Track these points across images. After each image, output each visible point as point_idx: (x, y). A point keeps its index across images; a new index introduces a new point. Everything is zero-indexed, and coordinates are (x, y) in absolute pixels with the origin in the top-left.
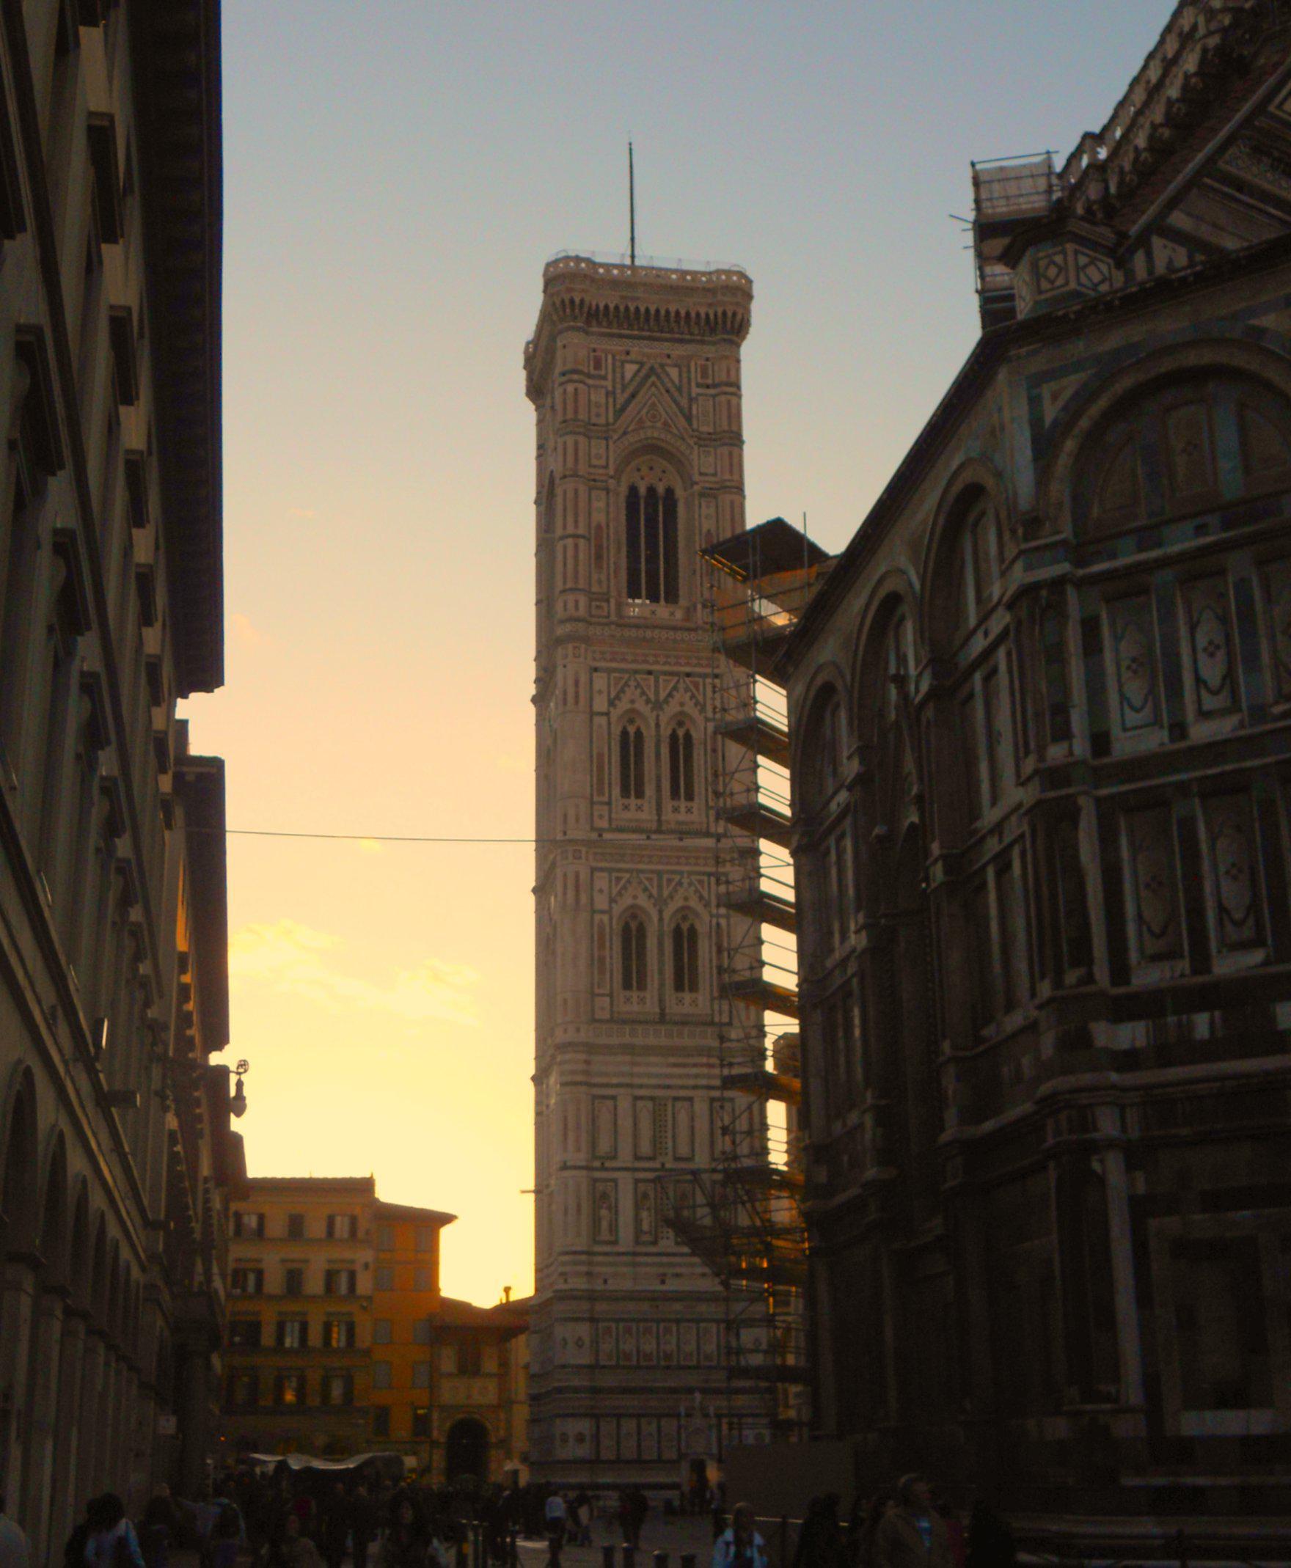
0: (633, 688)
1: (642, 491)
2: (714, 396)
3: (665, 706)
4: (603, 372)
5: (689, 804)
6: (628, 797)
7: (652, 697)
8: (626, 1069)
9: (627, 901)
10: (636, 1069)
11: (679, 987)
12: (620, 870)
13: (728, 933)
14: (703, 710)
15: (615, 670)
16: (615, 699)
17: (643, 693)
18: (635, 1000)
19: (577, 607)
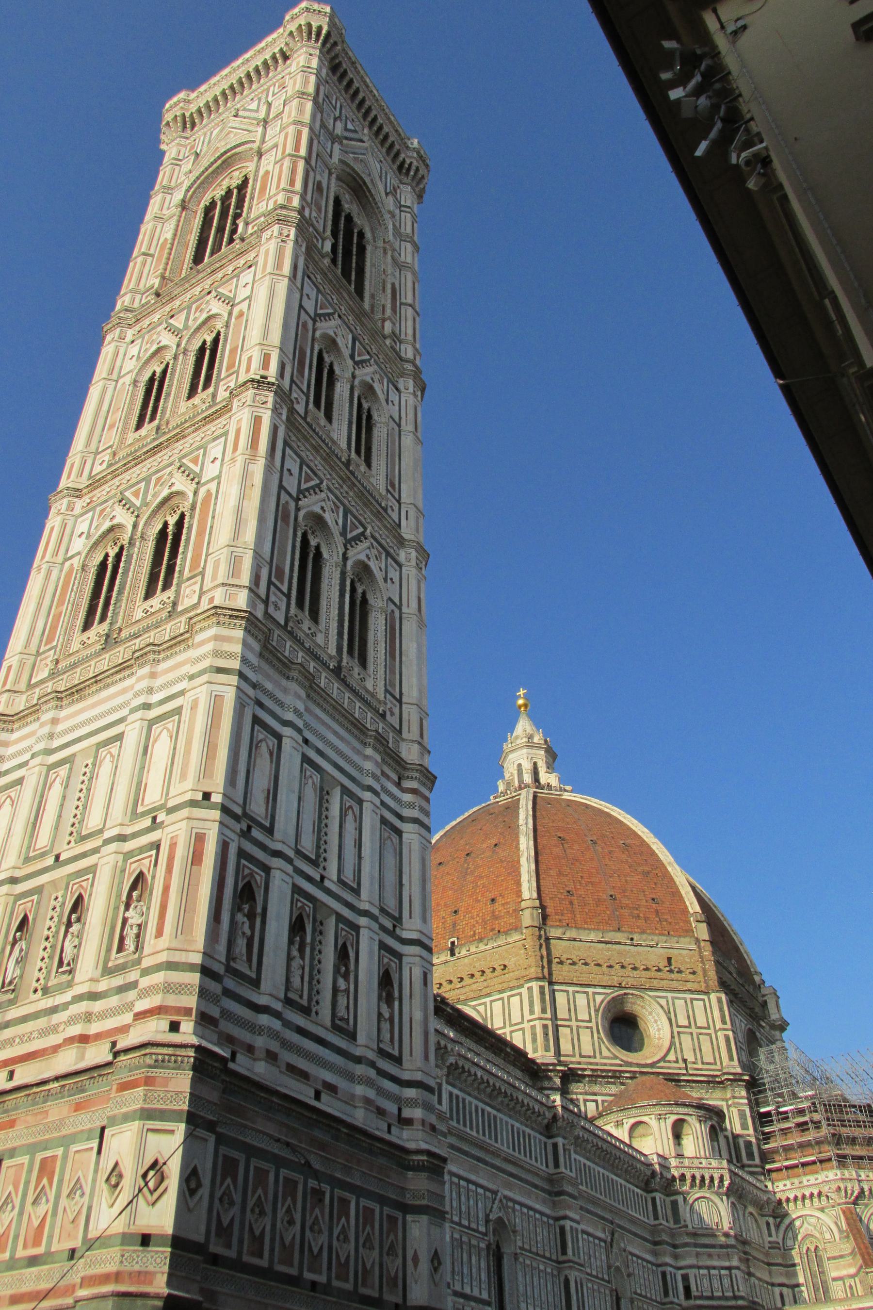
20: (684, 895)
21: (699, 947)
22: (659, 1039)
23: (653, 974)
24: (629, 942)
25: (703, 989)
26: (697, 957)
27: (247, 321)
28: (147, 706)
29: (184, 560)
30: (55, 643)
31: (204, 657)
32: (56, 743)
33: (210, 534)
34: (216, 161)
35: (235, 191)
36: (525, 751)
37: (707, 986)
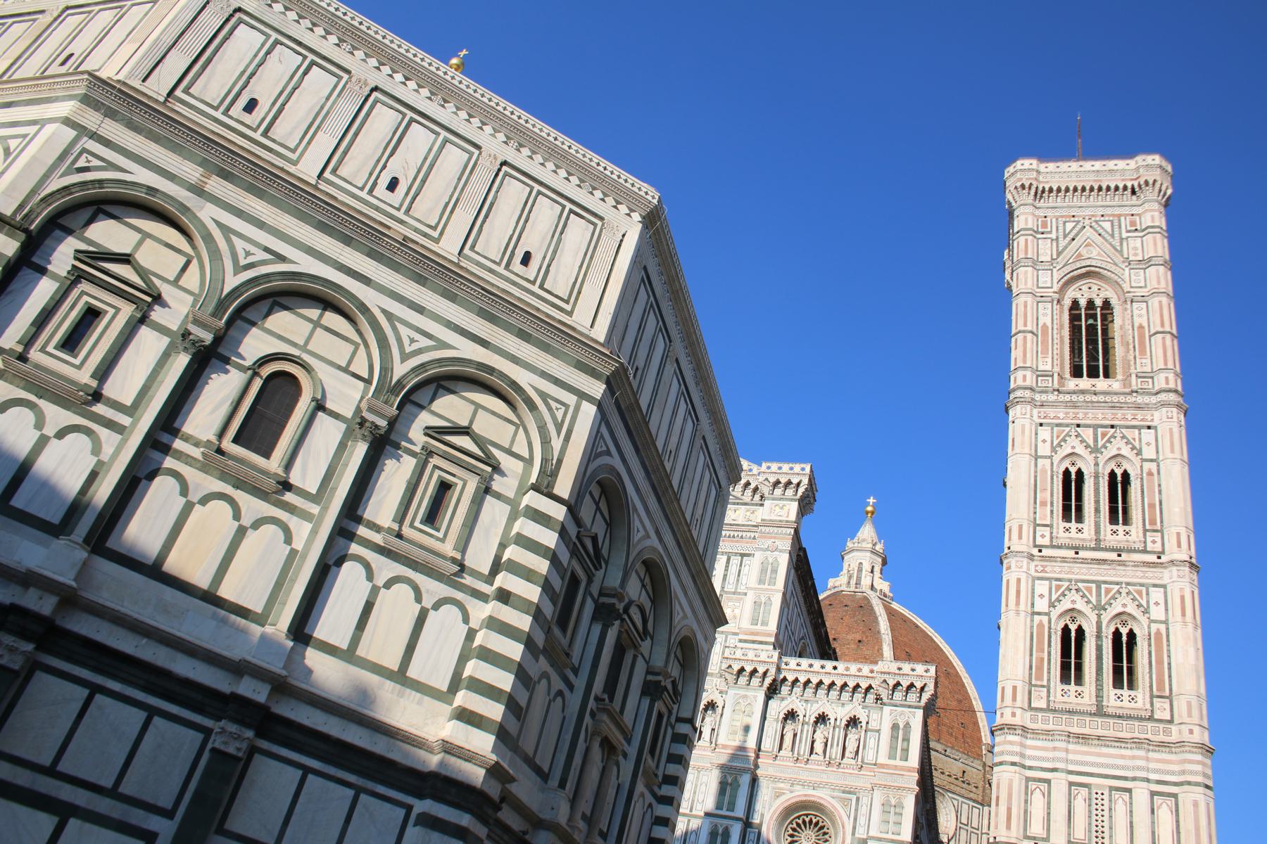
0: (1073, 437)
1: (1083, 303)
2: (1142, 237)
3: (1103, 450)
4: (1049, 230)
5: (1127, 528)
6: (1069, 521)
7: (1091, 443)
8: (1063, 755)
9: (1066, 605)
10: (1071, 757)
11: (1118, 683)
12: (1059, 580)
13: (1168, 636)
14: (1139, 453)
15: (1058, 425)
16: (1056, 446)
17: (1082, 442)
18: (1073, 694)
19: (1024, 380)
20: (981, 727)
21: (985, 770)
22: (946, 827)
23: (952, 780)
24: (943, 752)
25: (980, 799)
26: (981, 776)
27: (1159, 485)
28: (1148, 780)
29: (1151, 678)
30: (1045, 683)
31: (1196, 773)
32: (1071, 768)
33: (1170, 669)
34: (1081, 268)
35: (1099, 309)
36: (868, 554)
37: (983, 800)
